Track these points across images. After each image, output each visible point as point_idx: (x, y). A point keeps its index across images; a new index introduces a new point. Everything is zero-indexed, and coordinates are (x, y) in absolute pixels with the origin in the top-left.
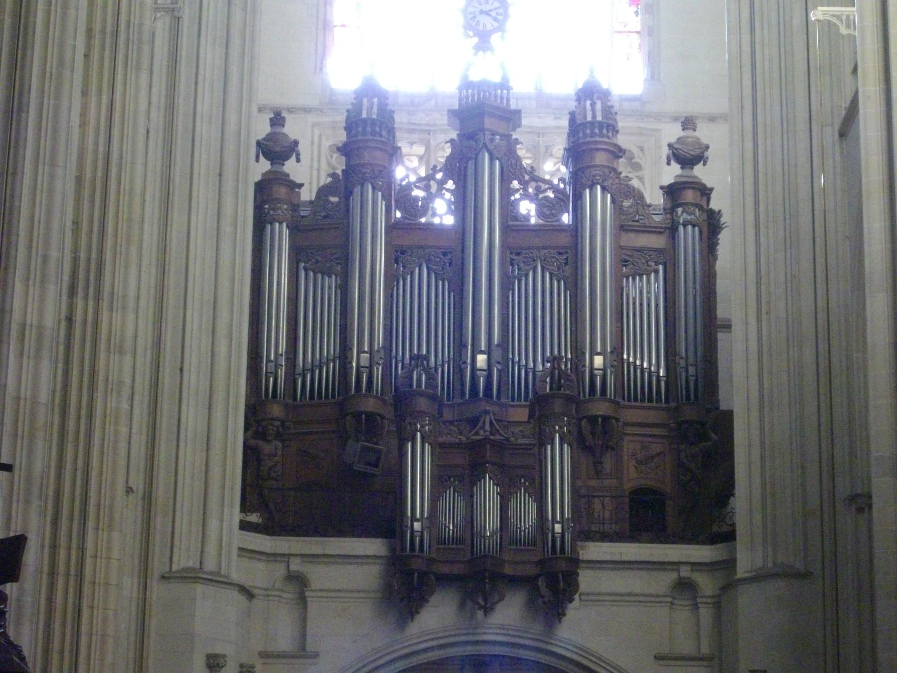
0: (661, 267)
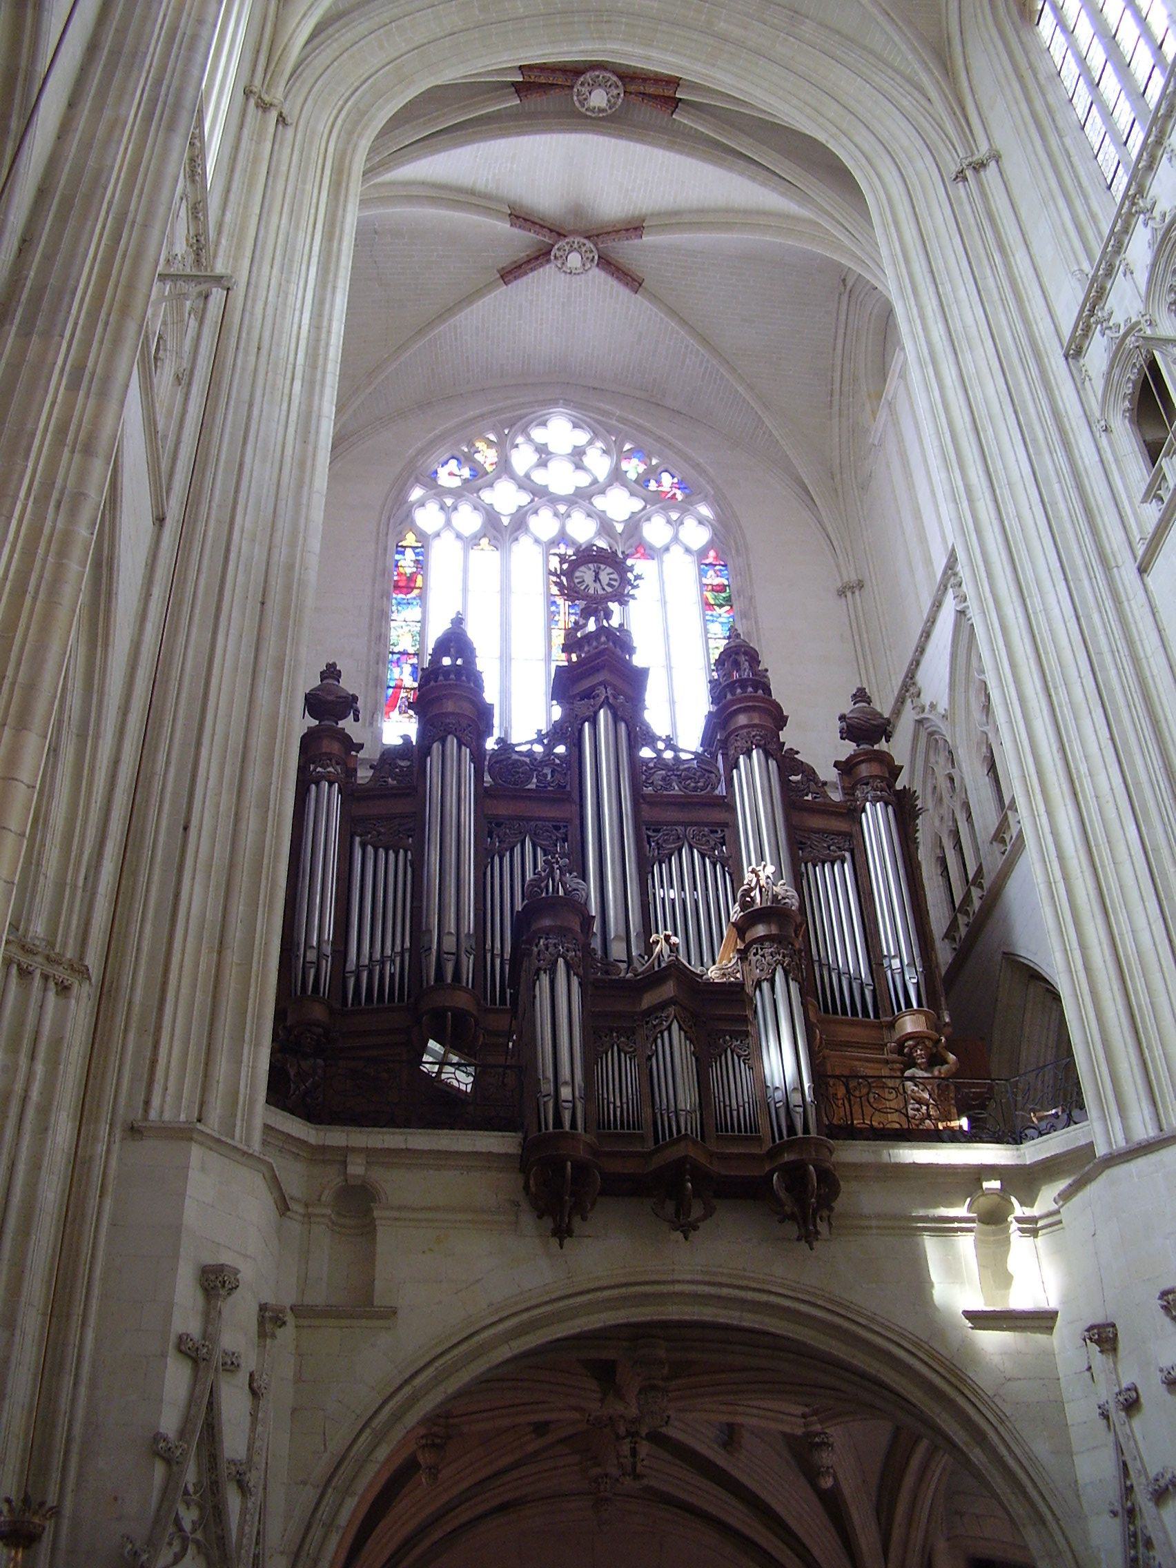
0: (847, 855)
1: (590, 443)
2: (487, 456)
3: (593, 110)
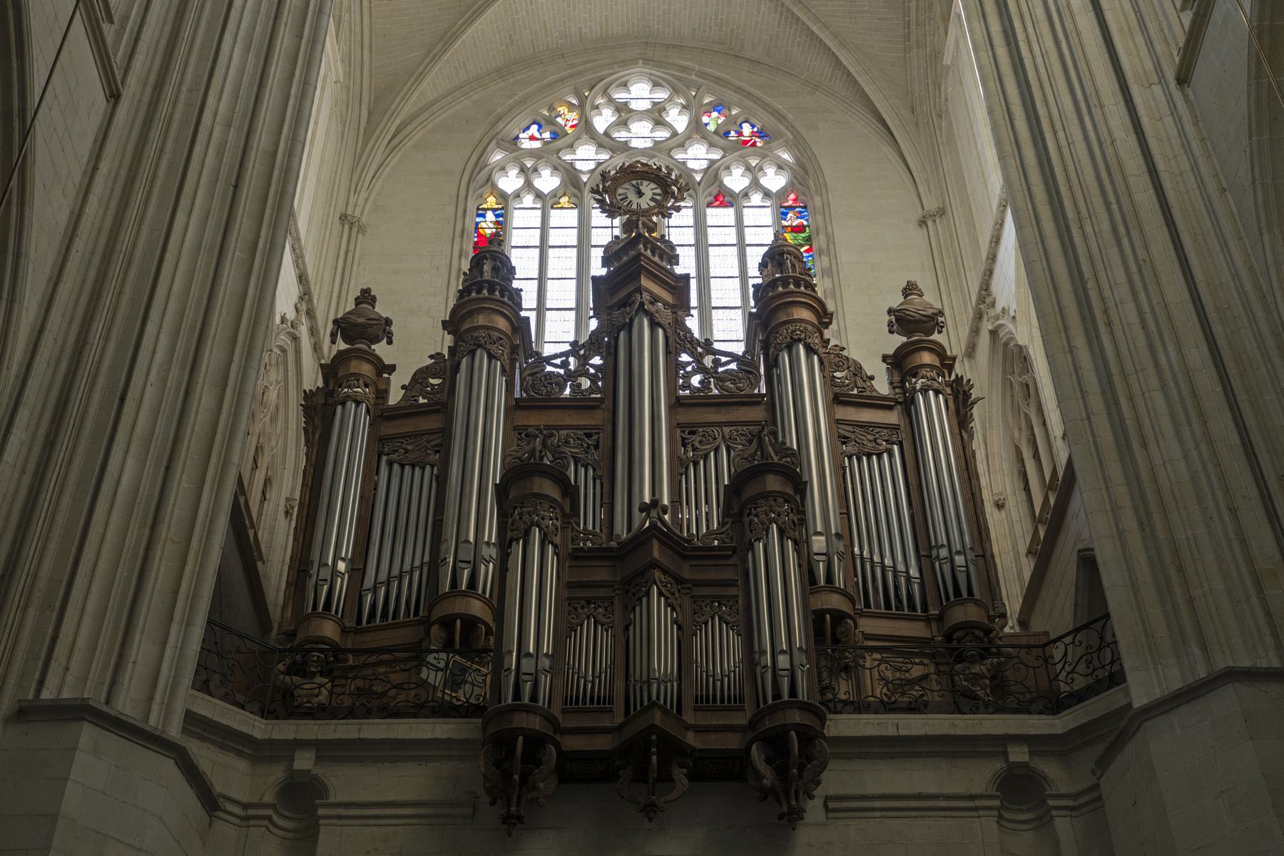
1: (670, 99)
2: (567, 118)
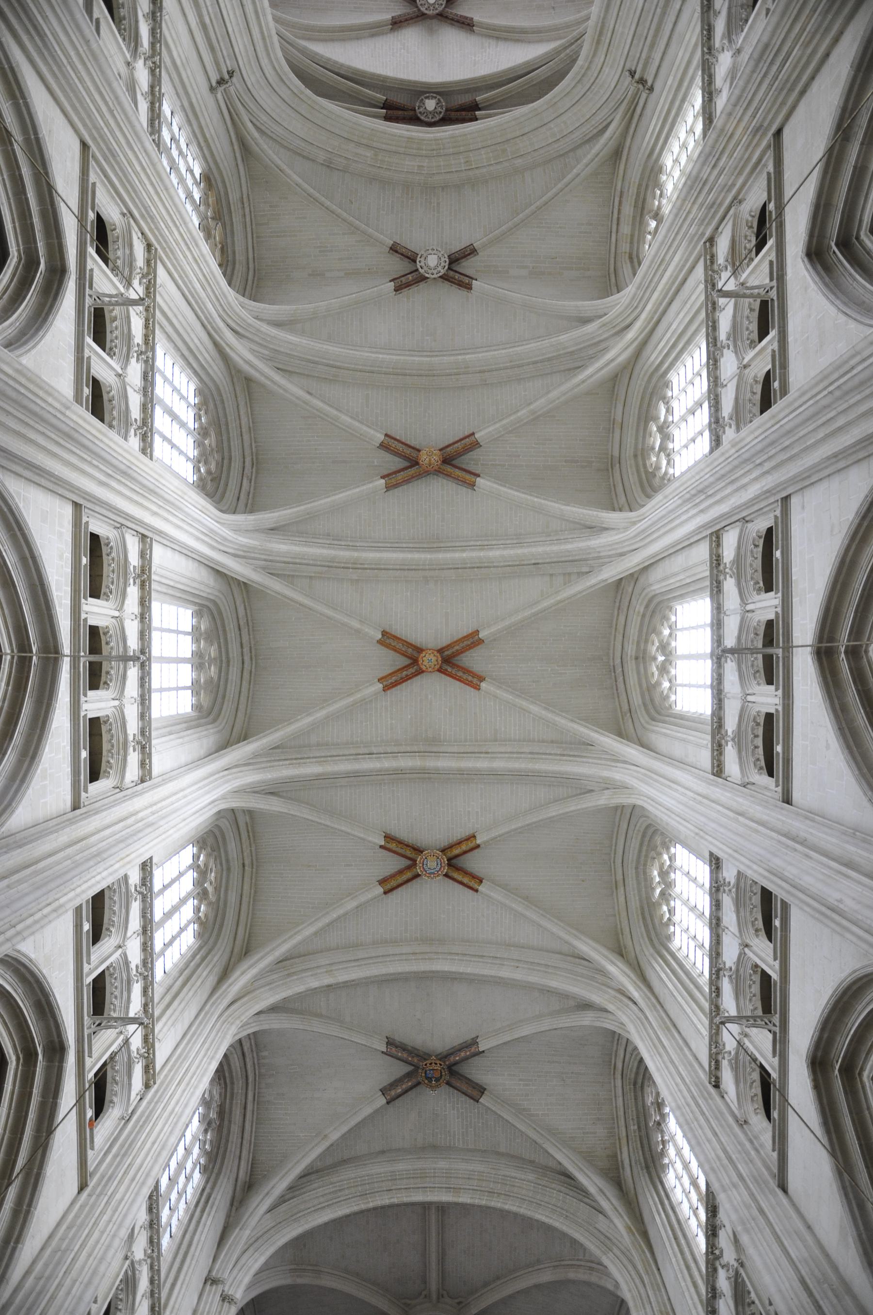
3: (433, 98)
